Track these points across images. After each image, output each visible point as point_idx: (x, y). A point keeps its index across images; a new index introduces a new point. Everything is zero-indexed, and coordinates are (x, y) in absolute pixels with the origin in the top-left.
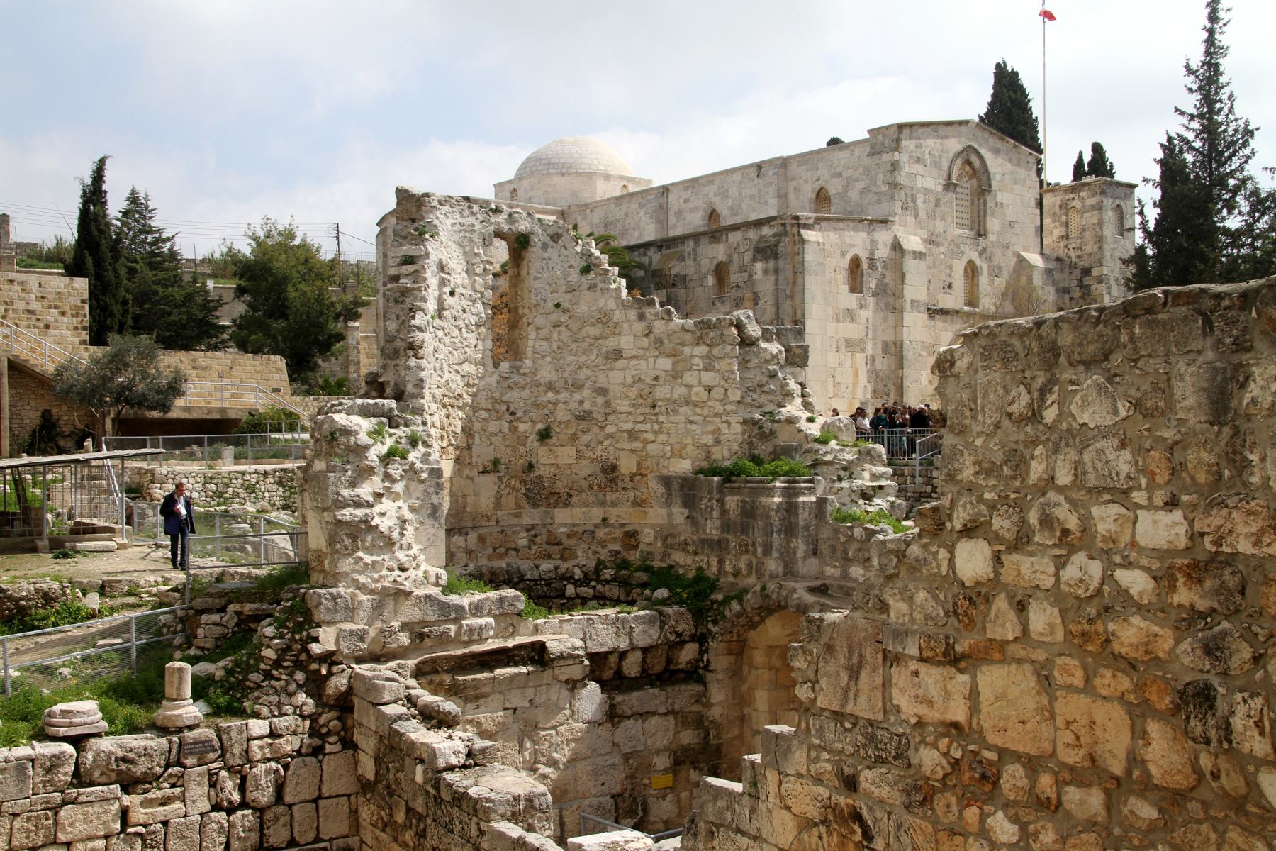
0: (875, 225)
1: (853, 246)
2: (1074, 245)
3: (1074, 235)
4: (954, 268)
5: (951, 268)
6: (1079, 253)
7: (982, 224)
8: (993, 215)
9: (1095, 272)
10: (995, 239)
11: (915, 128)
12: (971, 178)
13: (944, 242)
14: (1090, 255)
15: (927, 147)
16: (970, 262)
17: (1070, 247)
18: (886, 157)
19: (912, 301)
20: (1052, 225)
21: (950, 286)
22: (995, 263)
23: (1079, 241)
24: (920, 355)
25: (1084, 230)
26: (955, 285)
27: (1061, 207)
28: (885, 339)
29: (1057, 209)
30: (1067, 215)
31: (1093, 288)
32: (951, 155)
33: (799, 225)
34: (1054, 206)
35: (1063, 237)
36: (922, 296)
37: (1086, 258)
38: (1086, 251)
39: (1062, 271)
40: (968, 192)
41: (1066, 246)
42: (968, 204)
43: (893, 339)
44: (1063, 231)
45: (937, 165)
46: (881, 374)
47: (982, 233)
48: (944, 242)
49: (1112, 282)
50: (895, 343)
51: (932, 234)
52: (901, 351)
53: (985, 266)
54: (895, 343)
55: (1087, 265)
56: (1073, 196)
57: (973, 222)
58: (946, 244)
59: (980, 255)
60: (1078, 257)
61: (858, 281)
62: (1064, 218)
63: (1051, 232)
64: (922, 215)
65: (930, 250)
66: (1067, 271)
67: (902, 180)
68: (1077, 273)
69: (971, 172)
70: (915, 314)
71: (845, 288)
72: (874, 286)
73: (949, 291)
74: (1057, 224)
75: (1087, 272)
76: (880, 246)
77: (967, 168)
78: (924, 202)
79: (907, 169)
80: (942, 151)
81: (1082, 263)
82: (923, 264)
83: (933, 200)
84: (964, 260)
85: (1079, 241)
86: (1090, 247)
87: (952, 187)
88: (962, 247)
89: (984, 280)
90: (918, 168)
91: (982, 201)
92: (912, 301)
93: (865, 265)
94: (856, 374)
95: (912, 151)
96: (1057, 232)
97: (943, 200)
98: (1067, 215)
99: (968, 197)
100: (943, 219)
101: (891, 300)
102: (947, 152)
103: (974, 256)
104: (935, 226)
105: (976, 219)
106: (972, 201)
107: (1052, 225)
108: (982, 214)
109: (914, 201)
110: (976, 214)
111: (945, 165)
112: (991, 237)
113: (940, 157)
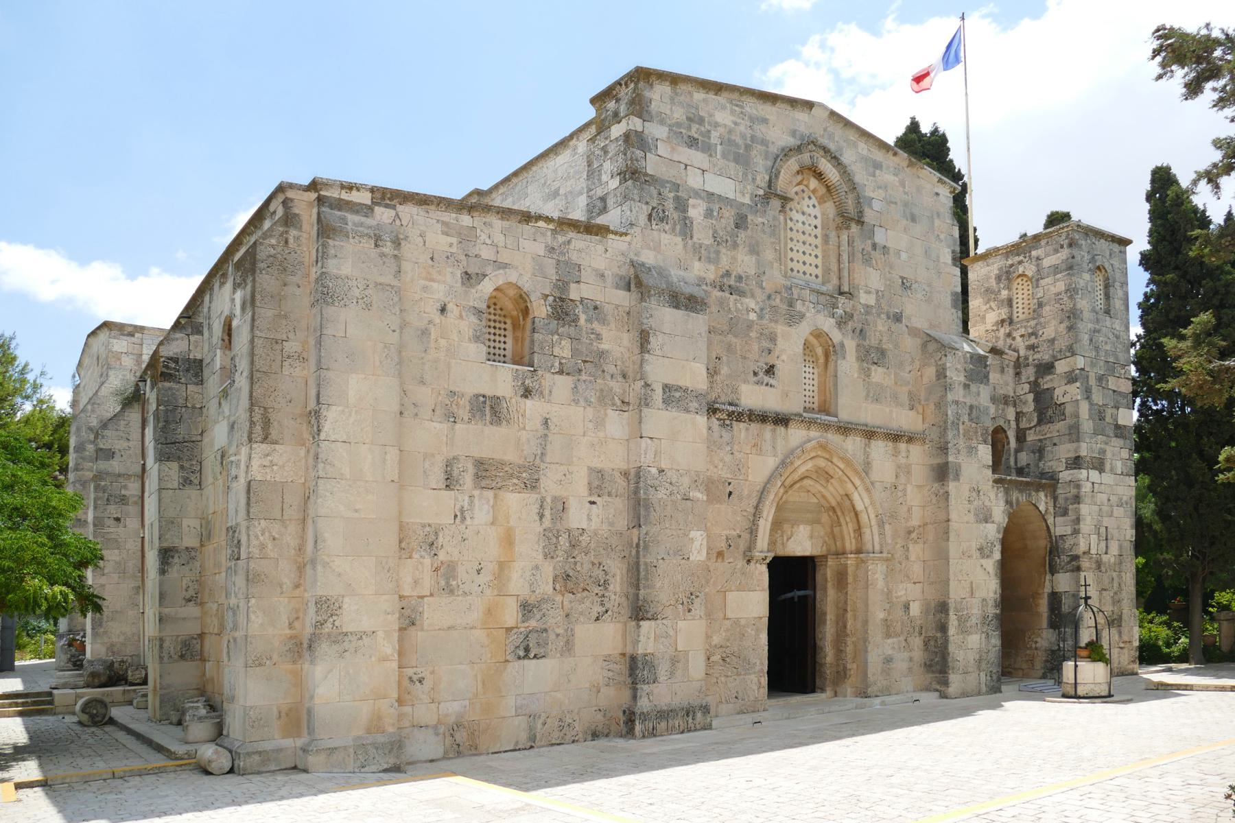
0: (572, 234)
1: (505, 266)
2: (1023, 331)
3: (1022, 317)
4: (780, 341)
5: (773, 339)
6: (1033, 340)
7: (845, 274)
8: (867, 261)
9: (1061, 367)
10: (872, 302)
11: (683, 87)
12: (821, 201)
13: (758, 291)
14: (1052, 341)
15: (716, 125)
16: (818, 334)
17: (1016, 334)
18: (617, 130)
19: (666, 388)
20: (984, 308)
21: (770, 370)
22: (872, 340)
23: (1033, 323)
24: (686, 499)
25: (1040, 305)
26: (781, 369)
27: (999, 278)
28: (599, 466)
29: (993, 282)
30: (1009, 289)
31: (1057, 392)
32: (774, 149)
33: (321, 200)
34: (990, 278)
35: (1003, 321)
36: (694, 376)
37: (1044, 347)
38: (1045, 337)
39: (1002, 371)
40: (818, 222)
41: (1009, 335)
42: (819, 241)
43: (624, 466)
44: (1003, 313)
45: (741, 158)
46: (584, 539)
47: (846, 289)
48: (758, 291)
49: (1092, 381)
50: (626, 474)
51: (728, 274)
52: (636, 491)
53: (851, 345)
54: (626, 474)
55: (1046, 357)
56: (1017, 259)
57: (827, 271)
58: (761, 296)
59: (841, 324)
60: (1032, 347)
61: (527, 343)
62: (1004, 293)
63: (984, 318)
64: (702, 235)
65: (721, 303)
66: (1010, 371)
67: (651, 165)
68: (1029, 373)
69: (822, 190)
70: (673, 413)
71: (477, 351)
72: (567, 353)
73: (766, 379)
74: (993, 304)
75: (1046, 368)
76: (586, 275)
77: (814, 183)
78: (709, 214)
79: (662, 149)
80: (753, 138)
81: (1037, 356)
82: (699, 322)
83: (729, 215)
84: (803, 330)
85: (1033, 323)
86: (1052, 328)
87: (776, 203)
88: (799, 306)
89: (848, 366)
90: (697, 157)
91: (844, 238)
92: (666, 388)
93: (540, 310)
94: (508, 540)
95: (679, 125)
96: (992, 317)
97: (755, 219)
98: (1009, 289)
99: (819, 231)
100: (754, 250)
101: (616, 386)
102: (764, 142)
103: (827, 324)
104: (734, 259)
105: (834, 267)
106: (826, 238)
107: (984, 308)
108: (845, 257)
109: (681, 206)
110: (833, 260)
111: (760, 165)
112: (865, 299)
113: (748, 148)
